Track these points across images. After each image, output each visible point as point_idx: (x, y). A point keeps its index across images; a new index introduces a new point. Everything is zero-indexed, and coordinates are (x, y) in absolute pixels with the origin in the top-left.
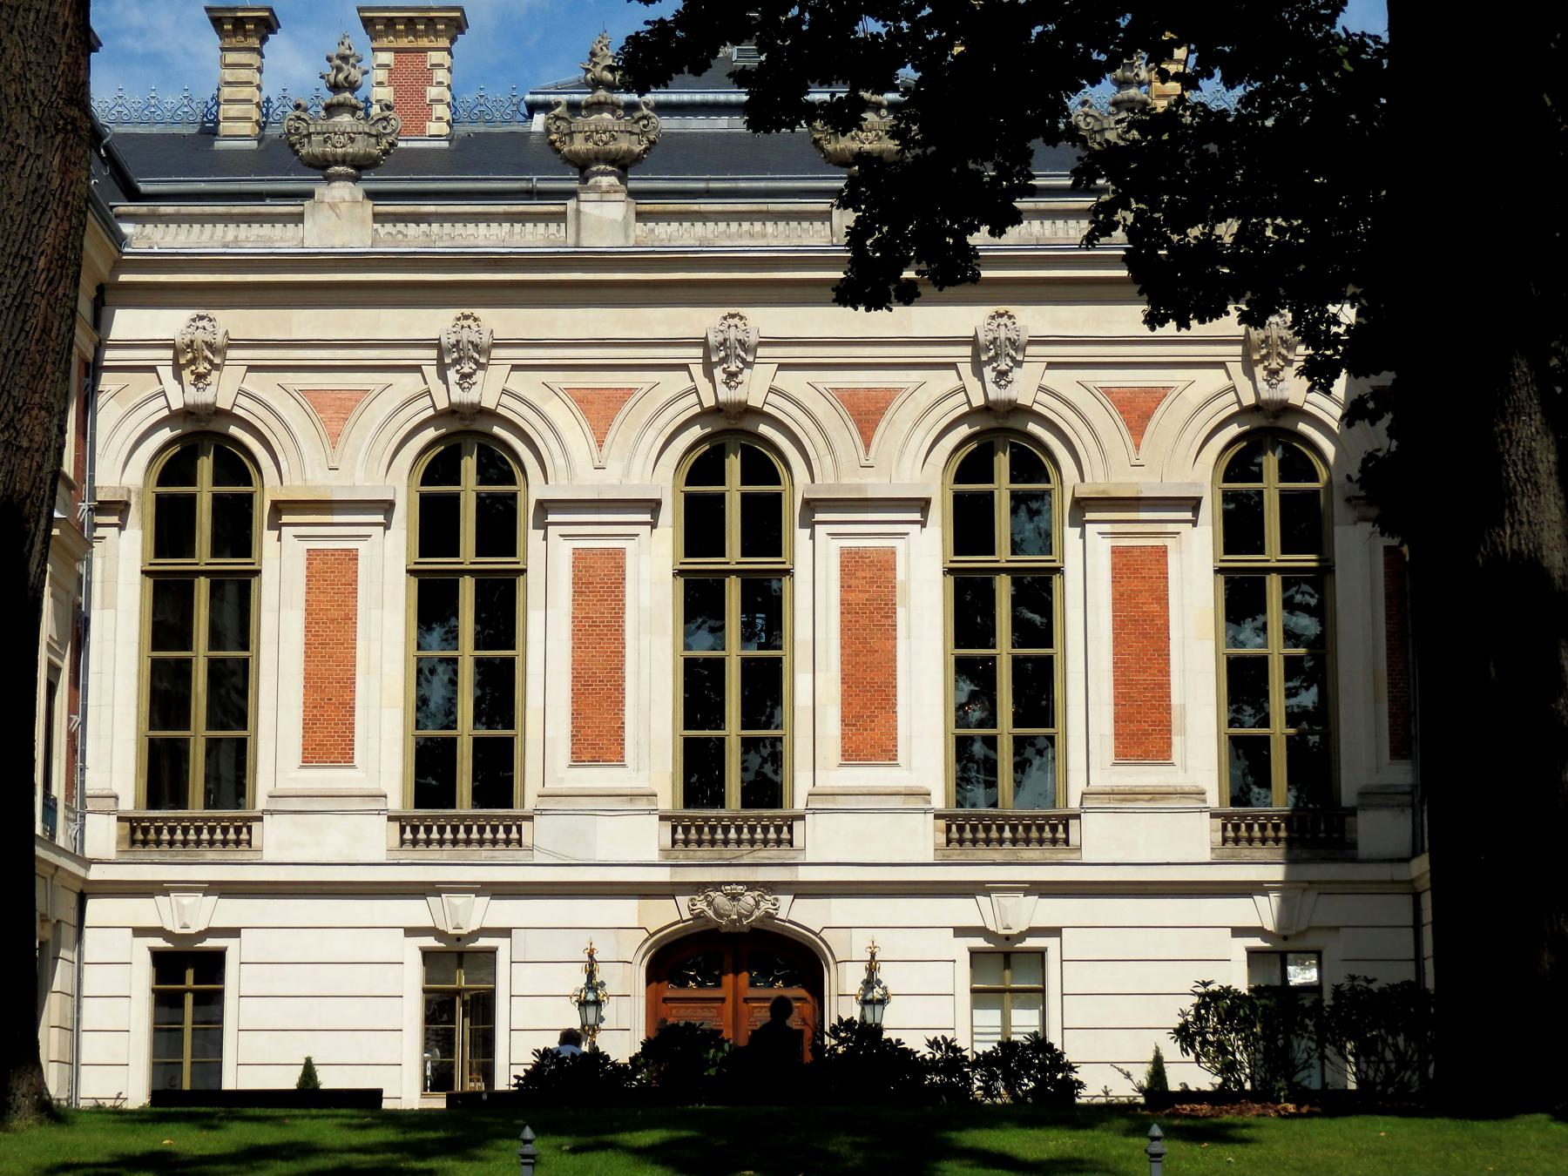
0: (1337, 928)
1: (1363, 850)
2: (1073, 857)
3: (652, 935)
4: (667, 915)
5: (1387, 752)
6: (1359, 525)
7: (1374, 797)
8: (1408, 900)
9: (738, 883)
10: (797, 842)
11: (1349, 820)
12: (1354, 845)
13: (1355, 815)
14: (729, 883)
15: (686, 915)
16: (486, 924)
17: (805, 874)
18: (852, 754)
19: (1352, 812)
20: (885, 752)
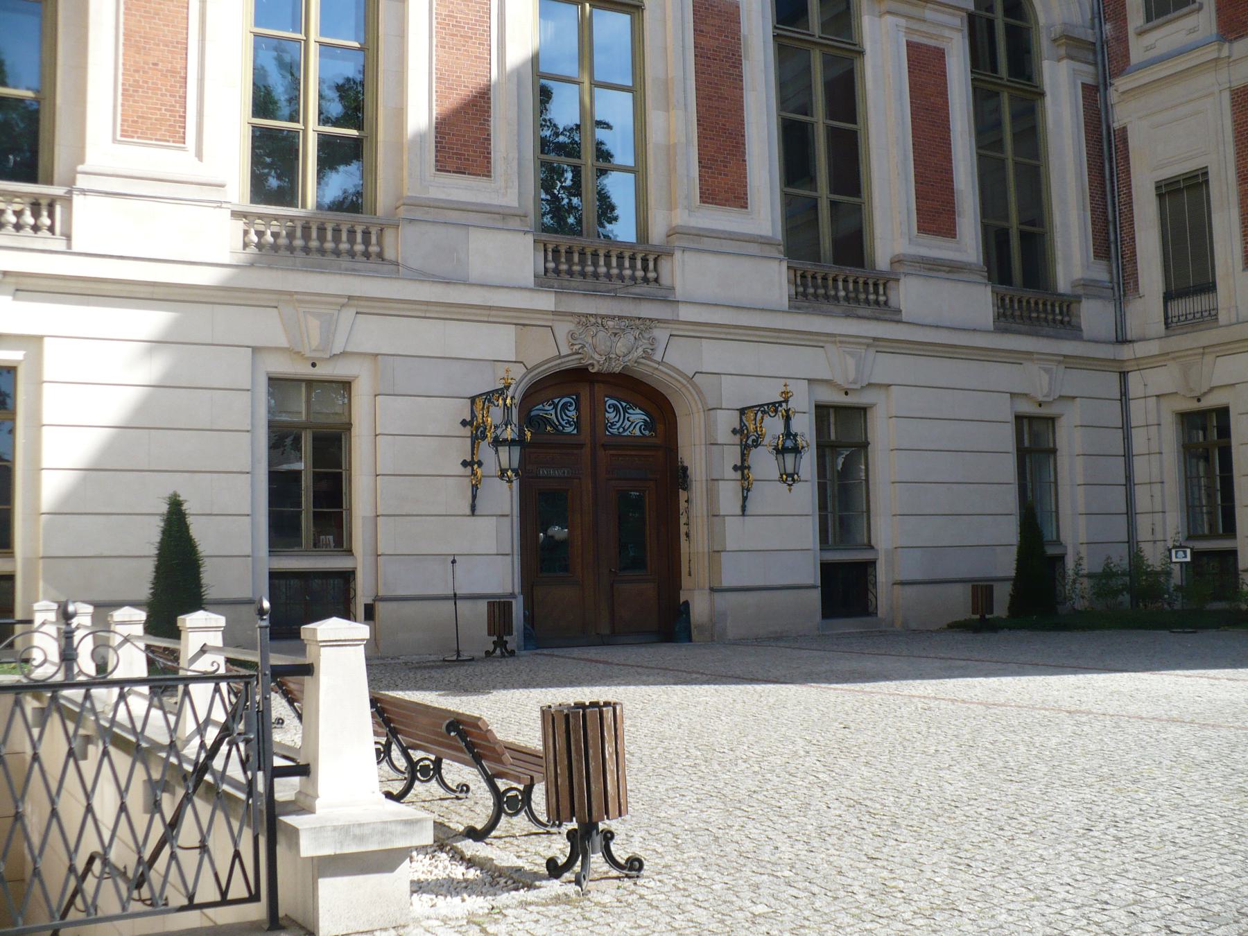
0: (1074, 398)
1: (1086, 334)
2: (897, 318)
3: (529, 371)
4: (549, 350)
5: (1092, 255)
6: (1065, 61)
7: (1089, 287)
8: (1115, 378)
9: (620, 318)
10: (665, 280)
11: (1073, 306)
12: (1079, 329)
13: (1080, 302)
14: (613, 318)
15: (565, 350)
16: (348, 349)
17: (686, 313)
18: (709, 196)
19: (1078, 299)
20: (736, 197)
